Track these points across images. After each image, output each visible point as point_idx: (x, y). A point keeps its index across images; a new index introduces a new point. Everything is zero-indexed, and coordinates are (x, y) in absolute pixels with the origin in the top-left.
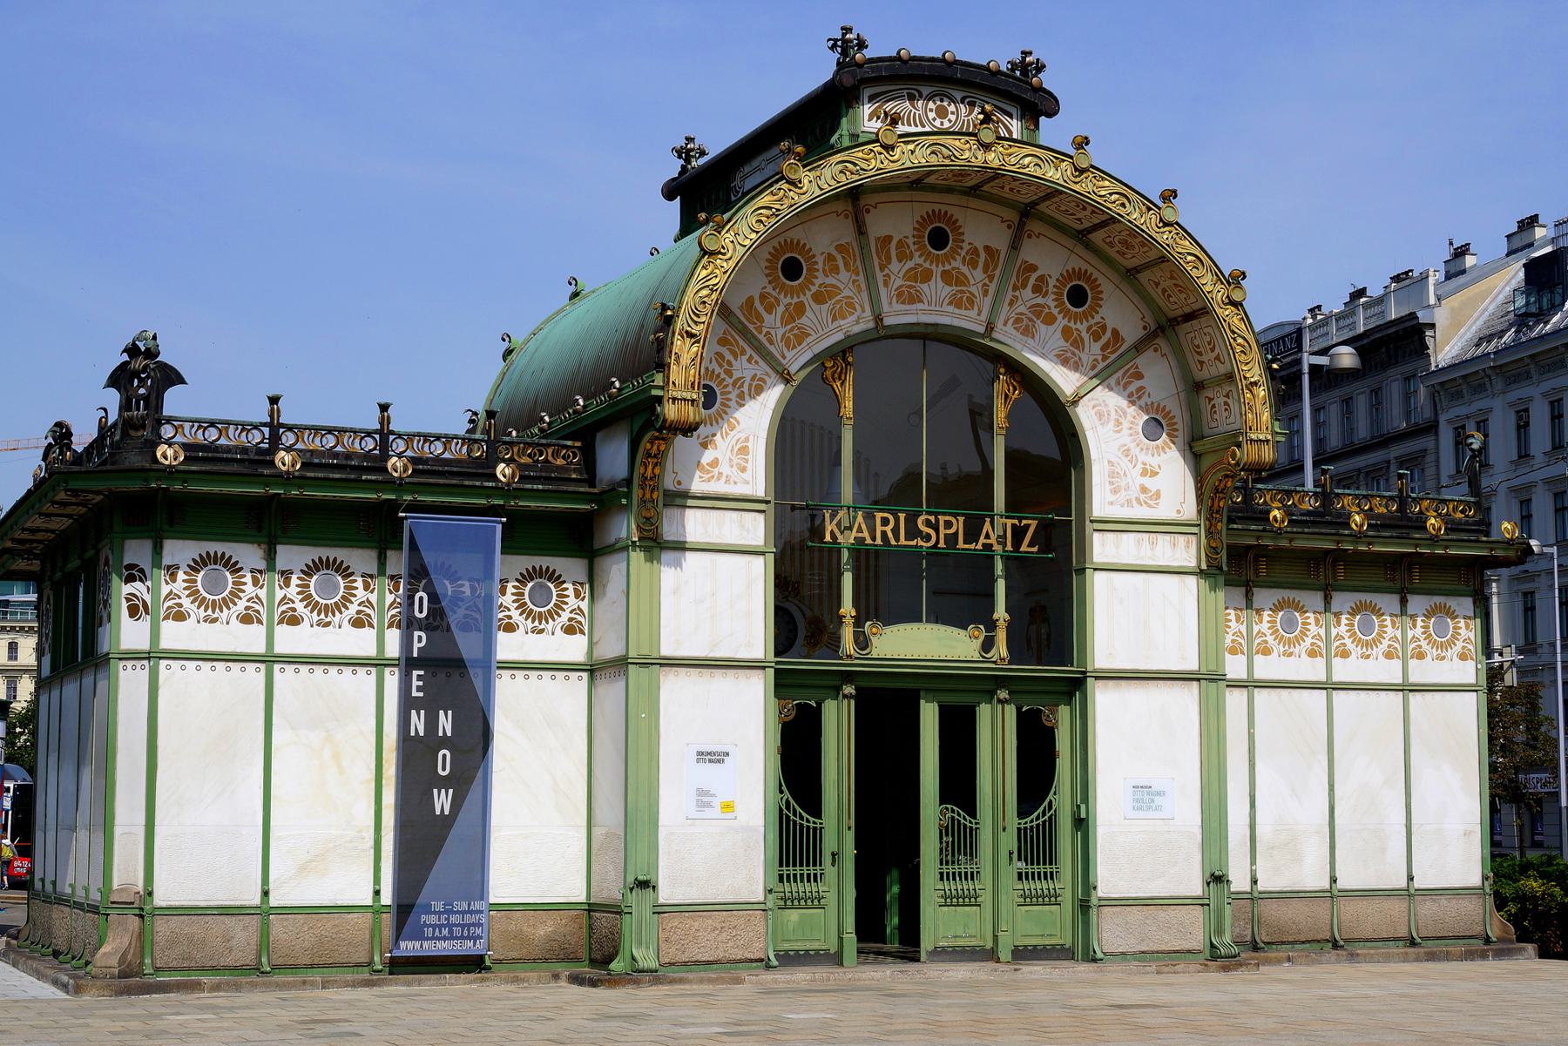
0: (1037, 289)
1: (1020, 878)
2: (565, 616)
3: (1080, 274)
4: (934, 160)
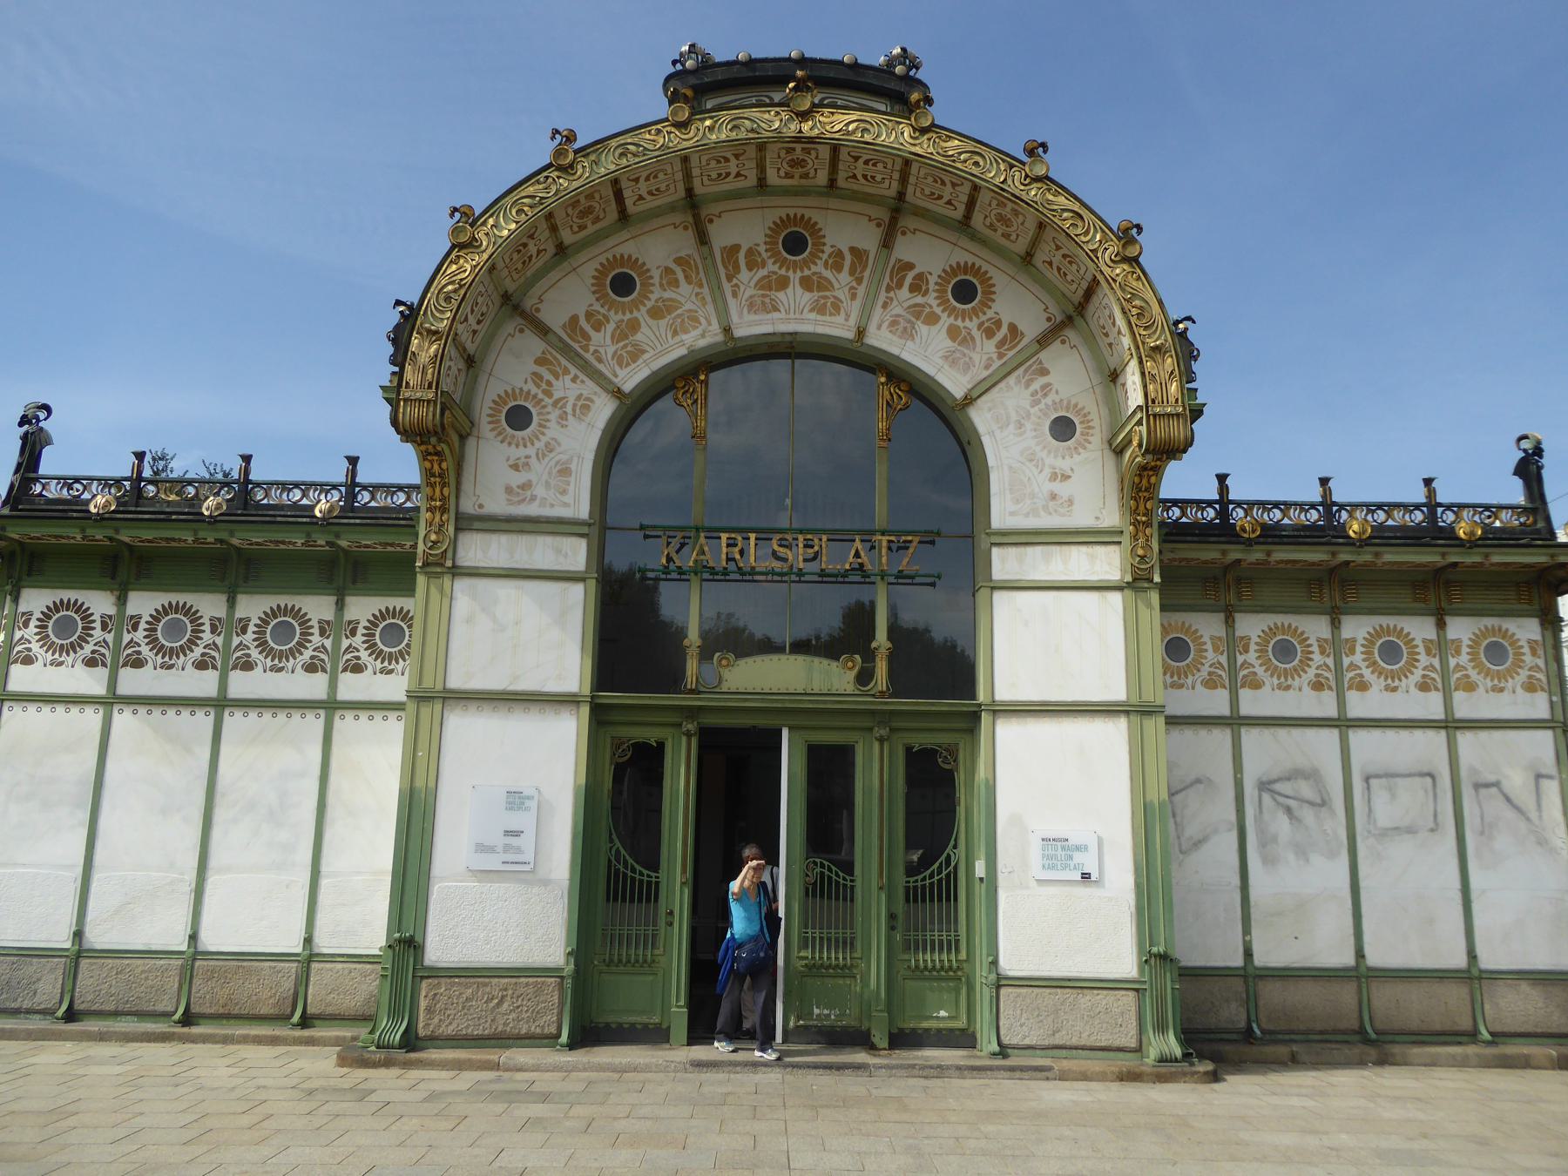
0: (915, 288)
3: (966, 269)
4: (733, 135)
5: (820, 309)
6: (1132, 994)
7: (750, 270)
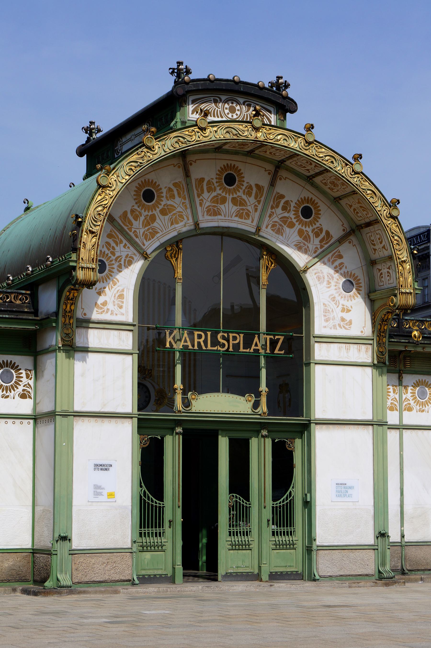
0: (284, 208)
1: (273, 534)
2: (21, 388)
3: (308, 200)
4: (228, 136)
5: (240, 215)
6: (372, 551)
7: (209, 192)
